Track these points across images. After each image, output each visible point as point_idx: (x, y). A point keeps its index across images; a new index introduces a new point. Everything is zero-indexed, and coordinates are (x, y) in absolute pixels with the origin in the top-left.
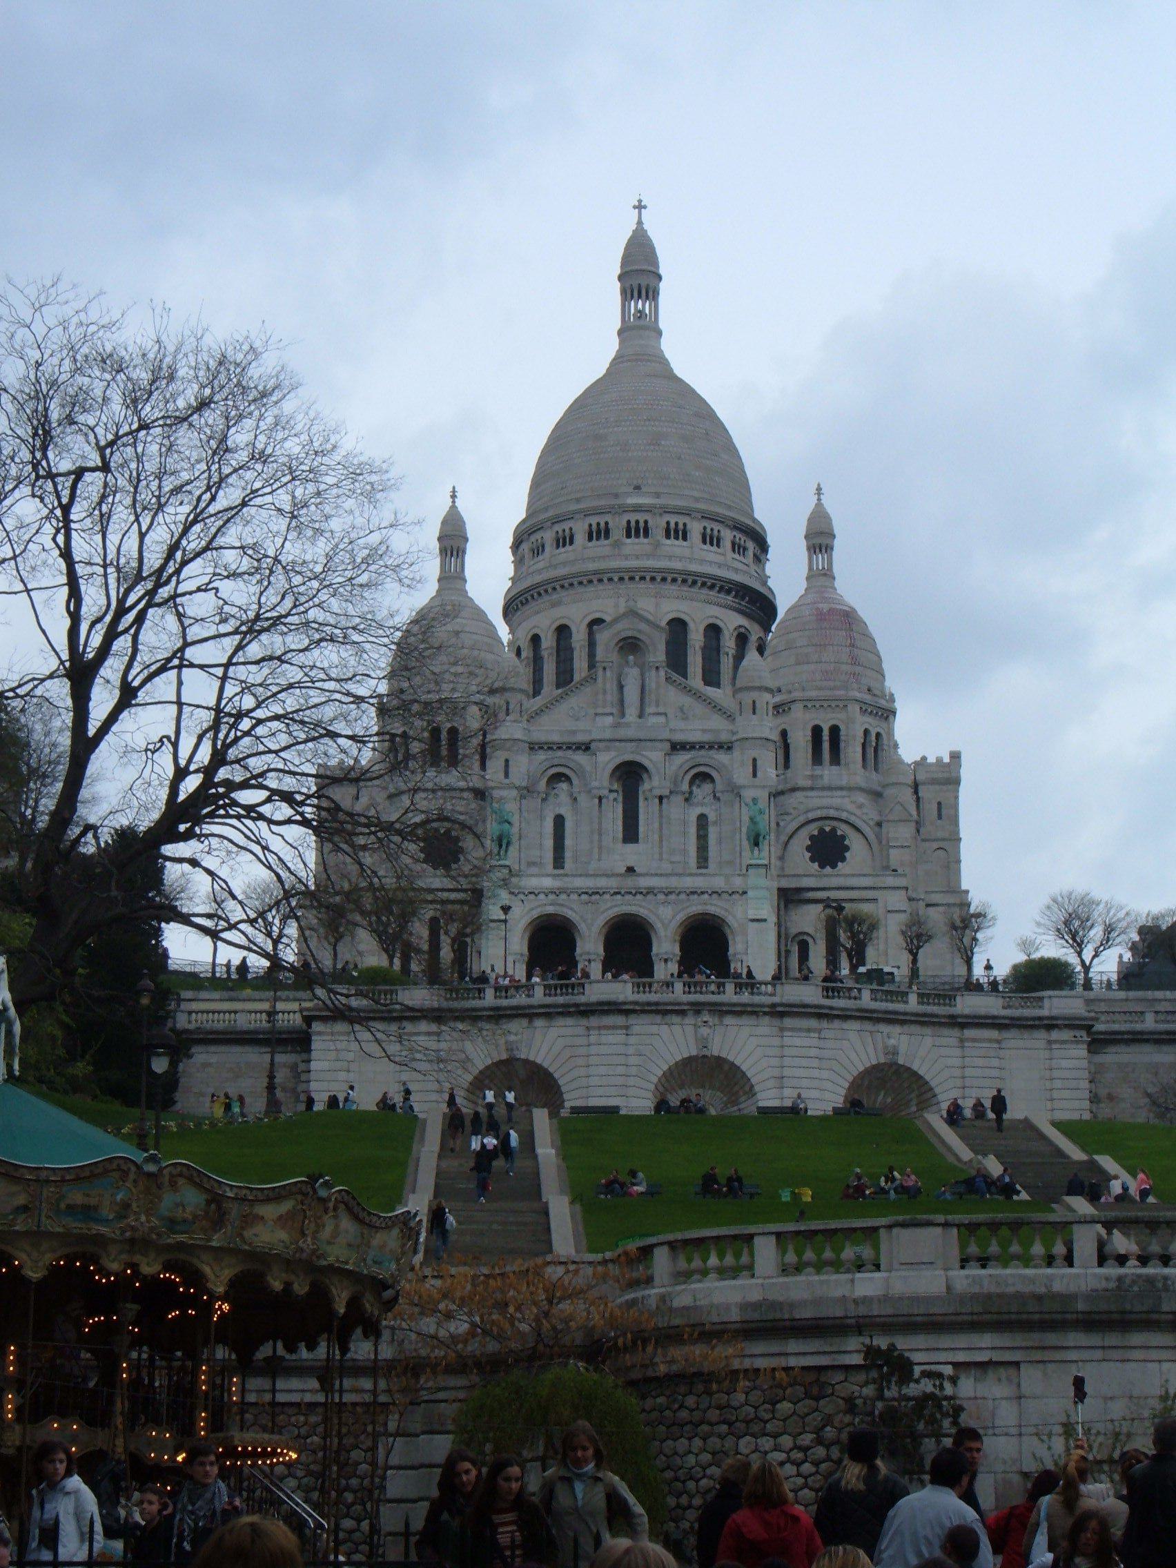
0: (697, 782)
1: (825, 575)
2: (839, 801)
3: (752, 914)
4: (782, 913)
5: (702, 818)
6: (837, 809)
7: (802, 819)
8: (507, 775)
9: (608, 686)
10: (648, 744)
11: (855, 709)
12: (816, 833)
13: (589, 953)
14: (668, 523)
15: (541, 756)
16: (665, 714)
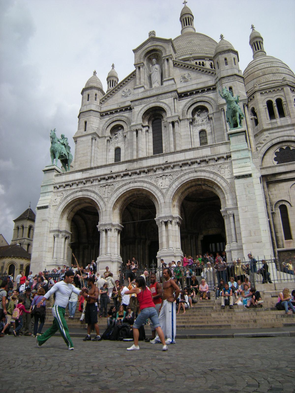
0: (197, 113)
1: (261, 51)
2: (288, 132)
3: (237, 172)
4: (266, 189)
5: (202, 132)
6: (288, 136)
7: (269, 144)
8: (85, 130)
9: (142, 75)
10: (163, 95)
11: (287, 89)
12: (278, 150)
13: (105, 225)
14: (196, 63)
15: (107, 118)
16: (173, 79)
